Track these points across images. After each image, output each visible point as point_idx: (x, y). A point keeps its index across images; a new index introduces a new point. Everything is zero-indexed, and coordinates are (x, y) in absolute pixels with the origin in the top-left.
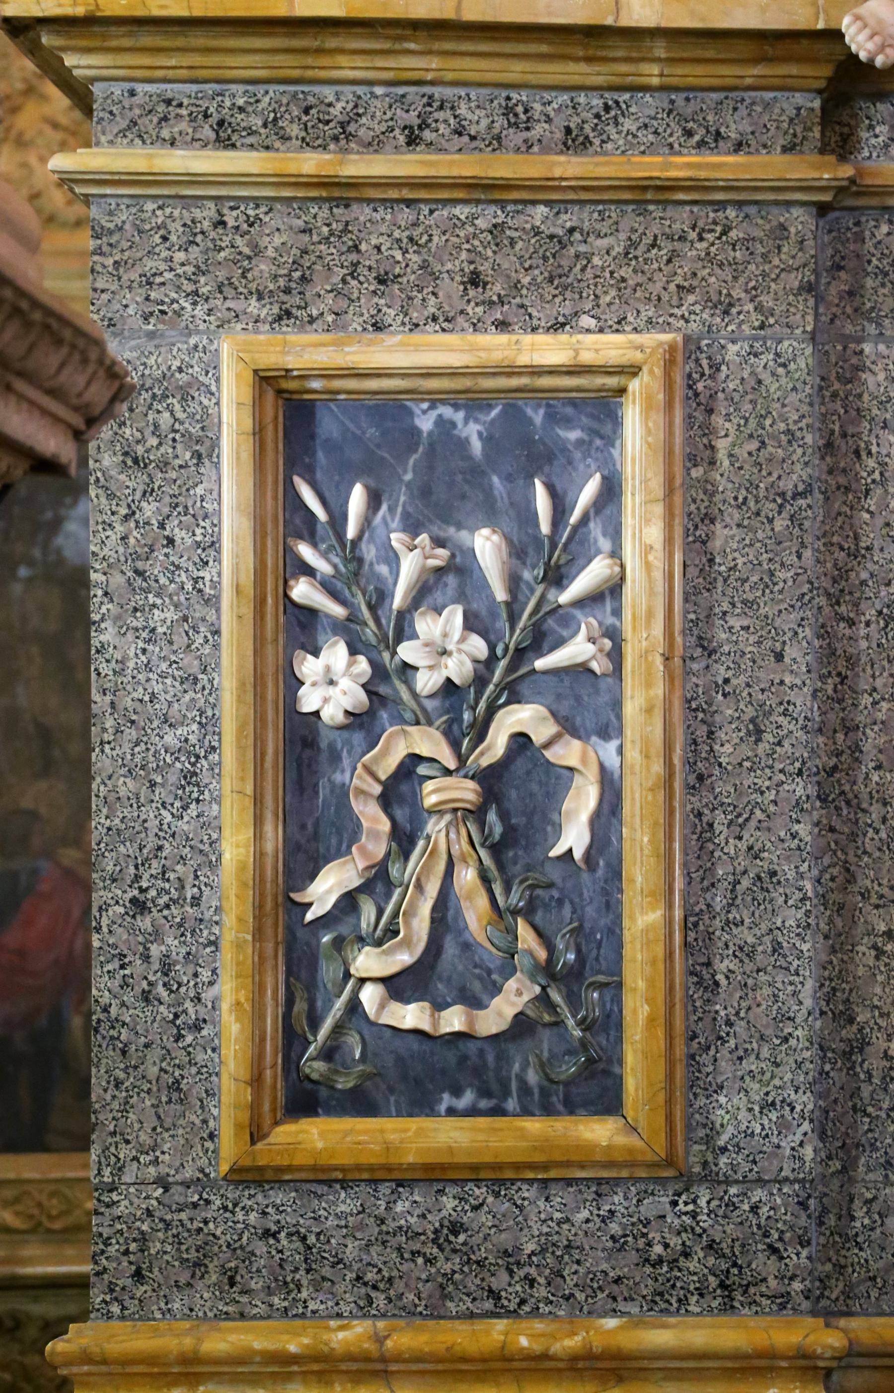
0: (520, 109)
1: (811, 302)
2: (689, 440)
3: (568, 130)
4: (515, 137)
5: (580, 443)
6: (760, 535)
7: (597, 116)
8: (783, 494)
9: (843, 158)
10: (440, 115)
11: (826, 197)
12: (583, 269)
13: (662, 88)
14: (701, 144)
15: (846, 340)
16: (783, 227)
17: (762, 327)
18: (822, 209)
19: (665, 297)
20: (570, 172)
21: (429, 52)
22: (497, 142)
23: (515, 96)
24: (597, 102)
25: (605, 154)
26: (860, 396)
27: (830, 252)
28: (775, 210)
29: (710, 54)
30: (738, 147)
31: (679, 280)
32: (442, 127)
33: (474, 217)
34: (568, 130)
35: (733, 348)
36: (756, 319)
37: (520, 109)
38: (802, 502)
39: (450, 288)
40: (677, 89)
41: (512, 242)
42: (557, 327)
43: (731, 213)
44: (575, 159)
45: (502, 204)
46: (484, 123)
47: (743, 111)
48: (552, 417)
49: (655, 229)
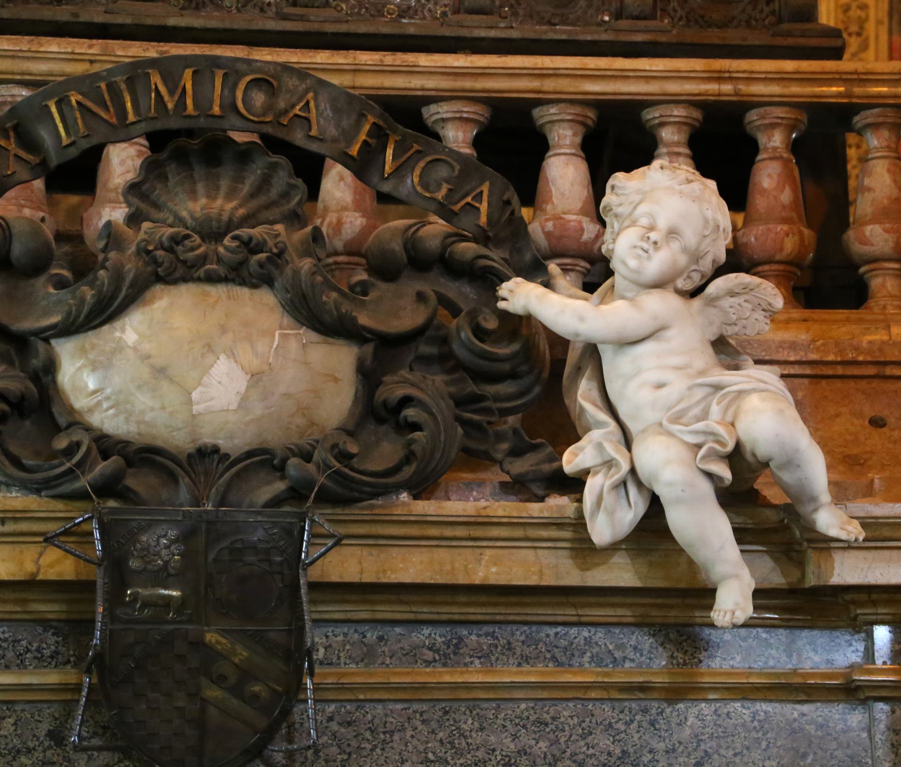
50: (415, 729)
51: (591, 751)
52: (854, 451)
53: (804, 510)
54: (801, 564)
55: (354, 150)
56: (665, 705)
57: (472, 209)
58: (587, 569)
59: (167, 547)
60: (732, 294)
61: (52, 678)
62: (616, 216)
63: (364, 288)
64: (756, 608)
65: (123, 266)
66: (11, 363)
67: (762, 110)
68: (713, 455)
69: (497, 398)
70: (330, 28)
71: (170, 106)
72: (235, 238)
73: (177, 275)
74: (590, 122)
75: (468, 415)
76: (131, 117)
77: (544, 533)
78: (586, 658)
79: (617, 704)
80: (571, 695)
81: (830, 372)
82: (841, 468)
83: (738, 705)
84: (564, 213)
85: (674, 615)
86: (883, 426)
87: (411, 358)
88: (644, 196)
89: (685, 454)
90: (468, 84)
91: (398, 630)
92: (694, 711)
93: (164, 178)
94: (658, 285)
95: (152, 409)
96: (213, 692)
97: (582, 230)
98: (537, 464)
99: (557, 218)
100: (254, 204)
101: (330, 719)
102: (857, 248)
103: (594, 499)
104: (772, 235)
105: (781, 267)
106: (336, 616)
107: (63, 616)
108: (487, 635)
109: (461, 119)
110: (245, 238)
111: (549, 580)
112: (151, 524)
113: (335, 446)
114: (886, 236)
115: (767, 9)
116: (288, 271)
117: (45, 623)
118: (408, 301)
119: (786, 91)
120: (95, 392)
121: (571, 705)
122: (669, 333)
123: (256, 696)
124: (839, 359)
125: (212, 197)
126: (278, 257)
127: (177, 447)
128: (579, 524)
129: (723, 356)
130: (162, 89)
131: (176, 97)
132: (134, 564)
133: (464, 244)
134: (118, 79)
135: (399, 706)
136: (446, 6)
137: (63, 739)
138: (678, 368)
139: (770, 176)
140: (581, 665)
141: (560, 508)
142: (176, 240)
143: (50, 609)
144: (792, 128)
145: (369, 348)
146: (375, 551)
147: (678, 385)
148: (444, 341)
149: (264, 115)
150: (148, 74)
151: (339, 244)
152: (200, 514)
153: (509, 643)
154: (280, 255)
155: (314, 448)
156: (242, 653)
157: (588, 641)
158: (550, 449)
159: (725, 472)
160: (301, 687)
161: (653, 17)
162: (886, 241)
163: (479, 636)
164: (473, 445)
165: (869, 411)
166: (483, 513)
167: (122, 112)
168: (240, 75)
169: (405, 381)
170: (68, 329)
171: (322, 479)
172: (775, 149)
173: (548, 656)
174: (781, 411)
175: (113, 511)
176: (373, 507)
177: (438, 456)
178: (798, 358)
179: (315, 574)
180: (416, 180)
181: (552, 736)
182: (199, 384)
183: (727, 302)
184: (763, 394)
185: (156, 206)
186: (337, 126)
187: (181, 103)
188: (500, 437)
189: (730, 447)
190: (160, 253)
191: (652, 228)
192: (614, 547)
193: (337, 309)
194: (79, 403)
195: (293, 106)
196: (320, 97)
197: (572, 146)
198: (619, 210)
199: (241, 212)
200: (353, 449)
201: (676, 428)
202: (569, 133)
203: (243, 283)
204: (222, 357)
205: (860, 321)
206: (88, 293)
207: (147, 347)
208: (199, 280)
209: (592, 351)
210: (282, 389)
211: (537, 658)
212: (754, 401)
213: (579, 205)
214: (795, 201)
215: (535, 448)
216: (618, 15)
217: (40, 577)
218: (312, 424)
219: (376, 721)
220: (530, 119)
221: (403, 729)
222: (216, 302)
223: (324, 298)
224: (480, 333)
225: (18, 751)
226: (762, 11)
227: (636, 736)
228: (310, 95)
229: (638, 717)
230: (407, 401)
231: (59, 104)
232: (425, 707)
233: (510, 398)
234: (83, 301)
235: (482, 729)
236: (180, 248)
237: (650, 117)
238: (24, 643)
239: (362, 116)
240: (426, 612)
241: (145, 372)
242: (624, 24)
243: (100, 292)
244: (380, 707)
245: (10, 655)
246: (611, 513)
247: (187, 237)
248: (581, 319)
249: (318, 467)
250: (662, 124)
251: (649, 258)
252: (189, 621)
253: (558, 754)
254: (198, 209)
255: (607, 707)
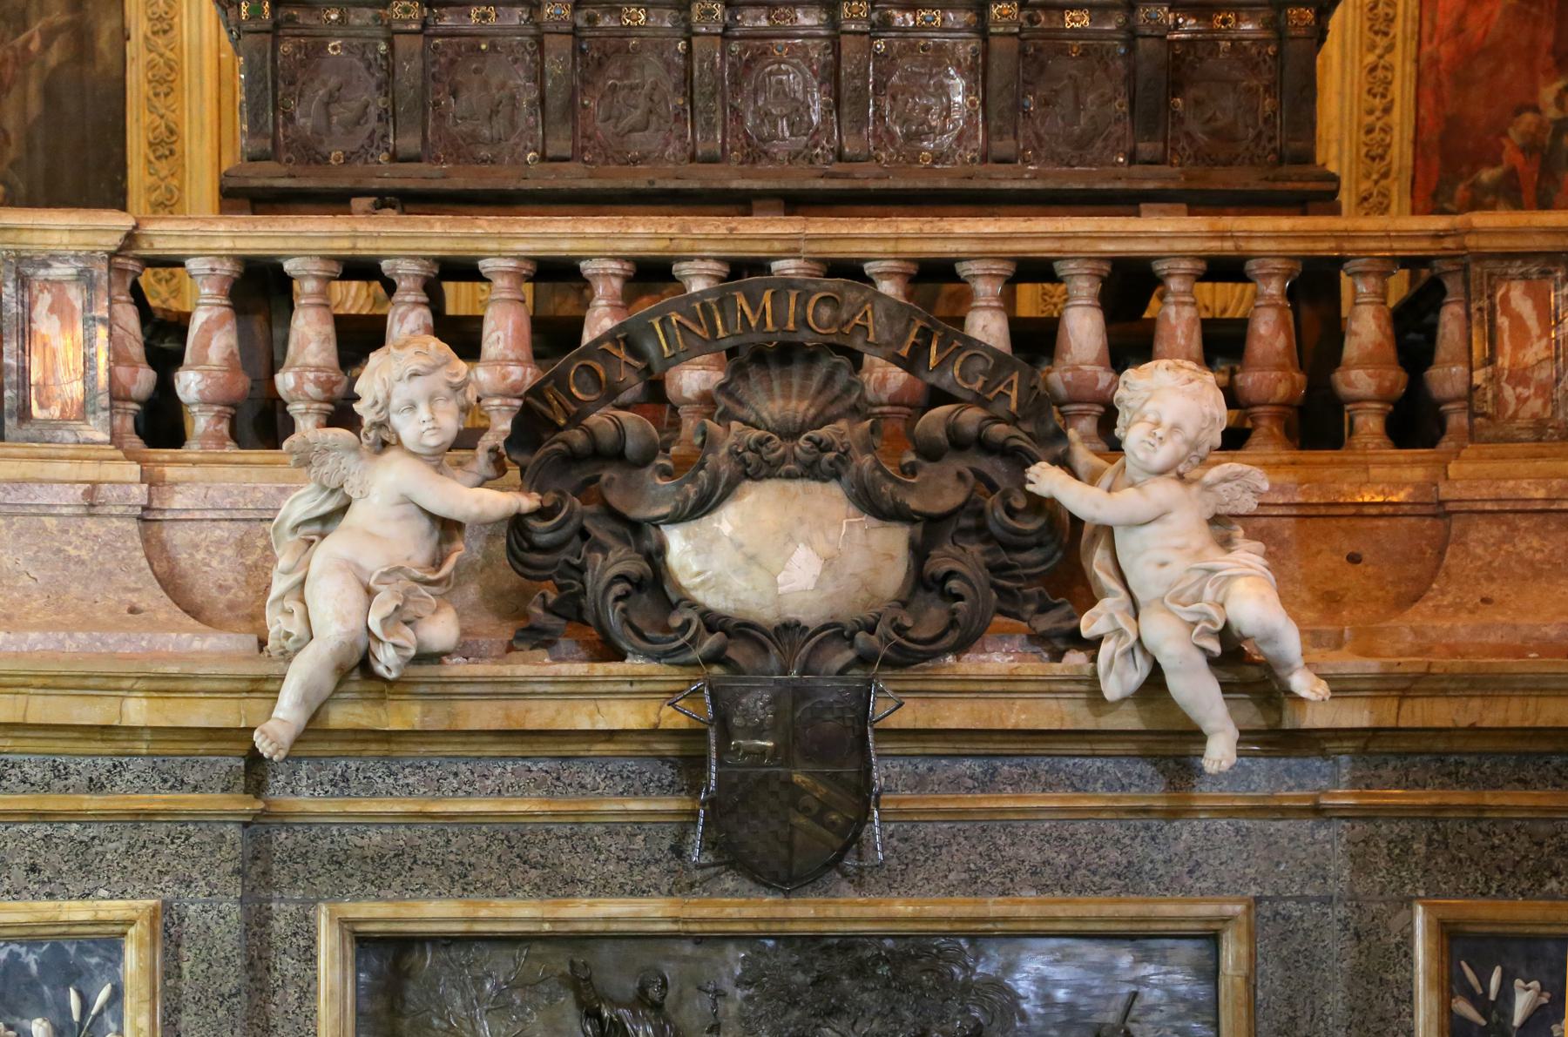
0: (61, 767)
1: (240, 880)
2: (165, 963)
3: (91, 780)
4: (59, 784)
5: (98, 965)
6: (209, 1020)
7: (109, 771)
8: (222, 995)
9: (258, 796)
10: (12, 771)
11: (248, 819)
12: (101, 861)
13: (148, 755)
14: (172, 787)
15: (261, 901)
16: (222, 836)
17: (210, 895)
18: (246, 825)
19: (151, 878)
20: (92, 806)
21: (7, 737)
22: (48, 786)
23: (58, 760)
24: (109, 763)
25: (114, 793)
26: (269, 935)
27: (251, 849)
28: (218, 826)
29: (177, 737)
30: (195, 788)
31: (159, 867)
32: (13, 778)
33: (32, 832)
34: (91, 780)
35: (192, 908)
36: (206, 890)
37: (61, 767)
38: (235, 1000)
39: (18, 874)
40: (157, 755)
41: (57, 845)
42: (85, 896)
43: (191, 827)
44: (95, 797)
45: (51, 824)
46: (40, 776)
47: (197, 768)
48: (81, 950)
49: (145, 836)
50: (959, 844)
51: (1103, 862)
52: (1331, 588)
53: (1281, 673)
54: (1279, 709)
55: (904, 352)
56: (1164, 823)
57: (1003, 396)
58: (1100, 716)
59: (763, 708)
60: (1225, 480)
61: (672, 805)
62: (1128, 408)
63: (911, 470)
64: (1238, 756)
65: (718, 467)
66: (628, 543)
67: (1260, 261)
68: (1205, 633)
69: (1025, 565)
70: (873, 185)
71: (753, 324)
72: (809, 439)
73: (763, 472)
74: (1105, 274)
75: (1001, 582)
76: (721, 334)
77: (1065, 687)
78: (1099, 785)
79: (1124, 823)
80: (1086, 816)
81: (1313, 512)
82: (1320, 606)
83: (1224, 822)
84: (1082, 364)
85: (1173, 749)
86: (1359, 561)
87: (953, 529)
88: (1152, 394)
89: (1182, 630)
90: (997, 247)
91: (944, 762)
92: (1187, 829)
93: (746, 377)
94: (1161, 473)
95: (746, 590)
96: (801, 820)
97: (1097, 380)
98: (1059, 622)
99: (1075, 368)
100: (822, 399)
101: (891, 836)
102: (1344, 390)
103: (1107, 662)
104: (1266, 382)
105: (1274, 409)
106: (894, 752)
107: (678, 753)
108: (1017, 765)
109: (990, 275)
110: (817, 439)
111: (1068, 725)
112: (749, 690)
113: (894, 619)
114: (1370, 380)
115: (1269, 147)
116: (853, 469)
117: (663, 758)
118: (949, 480)
119: (1283, 247)
120: (698, 574)
121: (1086, 823)
122: (1171, 517)
123: (834, 823)
124: (1322, 501)
125: (787, 397)
126: (844, 457)
127: (766, 621)
128: (1094, 680)
129: (1217, 527)
130: (747, 309)
131: (758, 316)
132: (737, 721)
133: (997, 426)
134: (709, 300)
135: (945, 826)
136: (975, 150)
137: (682, 852)
138: (1178, 548)
139: (1266, 323)
140: (1095, 790)
141: (1079, 667)
142: (761, 442)
143: (668, 748)
144: (1286, 277)
145: (919, 528)
146: (926, 703)
147: (1178, 565)
148: (981, 513)
149: (830, 327)
150: (735, 298)
151: (884, 397)
152: (788, 681)
153: (1035, 772)
154: (845, 453)
155: (878, 621)
156: (822, 791)
157: (1100, 770)
158: (1069, 607)
159: (1216, 648)
160: (869, 812)
161: (1163, 161)
162: (1369, 385)
163: (1010, 766)
164: (1006, 607)
165: (1348, 547)
166: (1015, 672)
167: (713, 329)
168: (810, 293)
169: (949, 555)
170: (675, 519)
171: (884, 651)
172: (1271, 296)
173: (1068, 783)
174: (1263, 597)
175: (719, 678)
176: (925, 669)
177: (977, 622)
178: (1286, 501)
179: (877, 726)
180: (956, 373)
181: (1070, 849)
182: (783, 569)
183: (1220, 488)
184: (1250, 579)
185: (740, 403)
186: (891, 332)
187: (763, 321)
188: (1027, 599)
189: (1220, 626)
190: (748, 455)
191: (1157, 424)
192: (1124, 700)
193: (893, 499)
194: (685, 581)
195: (854, 316)
196: (877, 307)
197: (1089, 296)
198: (1130, 404)
199: (812, 411)
200: (908, 622)
201: (1176, 607)
202: (1086, 284)
203: (816, 478)
204: (801, 545)
205: (1342, 463)
206: (691, 490)
207: (739, 537)
208: (780, 476)
209: (1107, 531)
210: (849, 571)
211: (1059, 784)
212: (1240, 586)
213: (1095, 355)
214: (1289, 346)
215: (1055, 606)
216: (1132, 158)
217: (661, 727)
218: (873, 596)
219: (928, 838)
220: (1052, 267)
221: (950, 844)
222: (795, 497)
223: (883, 490)
224: (1011, 512)
225: (649, 862)
226: (1264, 148)
227: (1140, 849)
228: (868, 306)
229: (1142, 834)
230: (951, 574)
231: (662, 322)
232: (967, 826)
233: (1037, 564)
234: (687, 498)
235: (1013, 844)
236: (764, 449)
237: (1158, 268)
238: (648, 774)
239: (911, 320)
240: (967, 748)
241: (738, 559)
242: (1137, 169)
243: (701, 489)
244: (930, 826)
245: (637, 784)
246: (1121, 676)
247: (769, 439)
248: (1098, 506)
249: (881, 639)
250: (1169, 275)
251: (1155, 451)
252: (778, 766)
253: (1075, 864)
254: (777, 411)
255: (1115, 825)
